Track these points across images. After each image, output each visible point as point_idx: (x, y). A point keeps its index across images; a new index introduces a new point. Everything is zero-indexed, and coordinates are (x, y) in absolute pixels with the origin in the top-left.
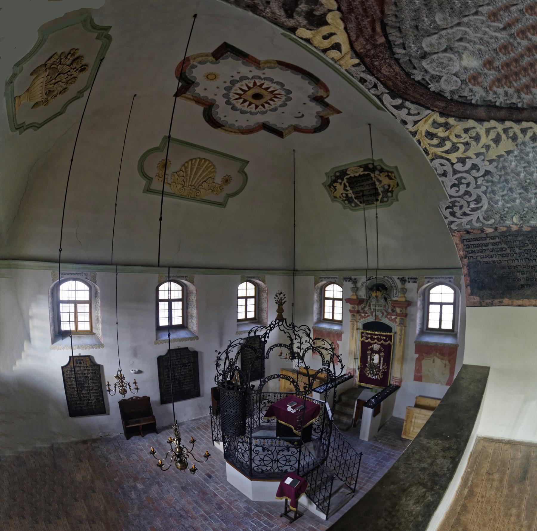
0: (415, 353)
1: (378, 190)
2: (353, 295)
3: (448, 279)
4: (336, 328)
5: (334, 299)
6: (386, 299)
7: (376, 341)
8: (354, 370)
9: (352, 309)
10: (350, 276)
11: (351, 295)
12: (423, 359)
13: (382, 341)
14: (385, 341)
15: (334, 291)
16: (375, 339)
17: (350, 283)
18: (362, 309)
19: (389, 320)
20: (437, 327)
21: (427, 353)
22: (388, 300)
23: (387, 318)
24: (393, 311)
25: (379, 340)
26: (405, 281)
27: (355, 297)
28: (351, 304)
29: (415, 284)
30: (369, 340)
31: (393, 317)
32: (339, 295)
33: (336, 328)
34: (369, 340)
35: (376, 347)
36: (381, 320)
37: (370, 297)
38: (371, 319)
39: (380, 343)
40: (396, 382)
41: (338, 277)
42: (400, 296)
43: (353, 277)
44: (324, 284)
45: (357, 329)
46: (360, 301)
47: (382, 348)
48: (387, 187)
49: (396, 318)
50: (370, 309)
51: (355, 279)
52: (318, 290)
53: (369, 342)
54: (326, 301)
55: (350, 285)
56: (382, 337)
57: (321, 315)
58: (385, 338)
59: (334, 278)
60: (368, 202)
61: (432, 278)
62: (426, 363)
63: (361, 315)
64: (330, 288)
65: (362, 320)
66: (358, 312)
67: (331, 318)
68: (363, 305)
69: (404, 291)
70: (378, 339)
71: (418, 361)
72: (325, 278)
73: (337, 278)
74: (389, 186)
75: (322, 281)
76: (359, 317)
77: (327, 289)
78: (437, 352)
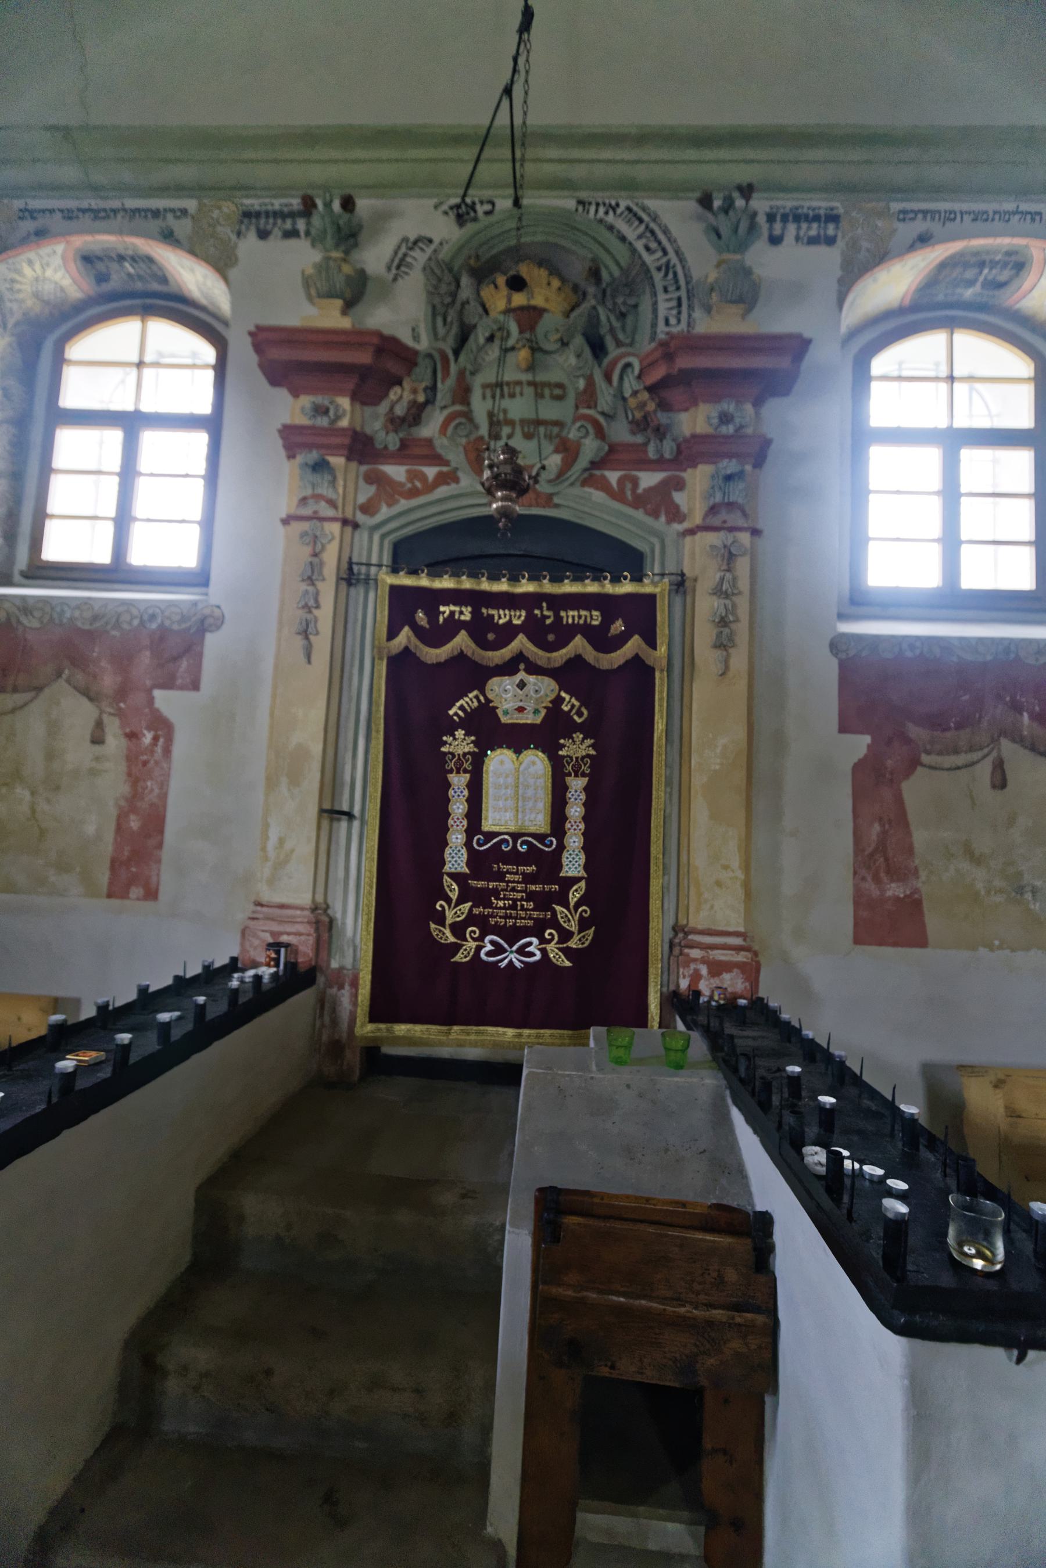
0: (844, 728)
7: (521, 643)
8: (324, 924)
13: (579, 644)
14: (601, 640)
16: (509, 632)
17: (301, 245)
19: (618, 495)
23: (604, 486)
30: (462, 641)
31: (648, 479)
34: (462, 641)
36: (548, 500)
40: (717, 969)
47: (569, 702)
50: (468, 415)
53: (460, 658)
56: (570, 616)
58: (596, 618)
59: (156, 214)
70: (535, 630)
76: (366, 493)
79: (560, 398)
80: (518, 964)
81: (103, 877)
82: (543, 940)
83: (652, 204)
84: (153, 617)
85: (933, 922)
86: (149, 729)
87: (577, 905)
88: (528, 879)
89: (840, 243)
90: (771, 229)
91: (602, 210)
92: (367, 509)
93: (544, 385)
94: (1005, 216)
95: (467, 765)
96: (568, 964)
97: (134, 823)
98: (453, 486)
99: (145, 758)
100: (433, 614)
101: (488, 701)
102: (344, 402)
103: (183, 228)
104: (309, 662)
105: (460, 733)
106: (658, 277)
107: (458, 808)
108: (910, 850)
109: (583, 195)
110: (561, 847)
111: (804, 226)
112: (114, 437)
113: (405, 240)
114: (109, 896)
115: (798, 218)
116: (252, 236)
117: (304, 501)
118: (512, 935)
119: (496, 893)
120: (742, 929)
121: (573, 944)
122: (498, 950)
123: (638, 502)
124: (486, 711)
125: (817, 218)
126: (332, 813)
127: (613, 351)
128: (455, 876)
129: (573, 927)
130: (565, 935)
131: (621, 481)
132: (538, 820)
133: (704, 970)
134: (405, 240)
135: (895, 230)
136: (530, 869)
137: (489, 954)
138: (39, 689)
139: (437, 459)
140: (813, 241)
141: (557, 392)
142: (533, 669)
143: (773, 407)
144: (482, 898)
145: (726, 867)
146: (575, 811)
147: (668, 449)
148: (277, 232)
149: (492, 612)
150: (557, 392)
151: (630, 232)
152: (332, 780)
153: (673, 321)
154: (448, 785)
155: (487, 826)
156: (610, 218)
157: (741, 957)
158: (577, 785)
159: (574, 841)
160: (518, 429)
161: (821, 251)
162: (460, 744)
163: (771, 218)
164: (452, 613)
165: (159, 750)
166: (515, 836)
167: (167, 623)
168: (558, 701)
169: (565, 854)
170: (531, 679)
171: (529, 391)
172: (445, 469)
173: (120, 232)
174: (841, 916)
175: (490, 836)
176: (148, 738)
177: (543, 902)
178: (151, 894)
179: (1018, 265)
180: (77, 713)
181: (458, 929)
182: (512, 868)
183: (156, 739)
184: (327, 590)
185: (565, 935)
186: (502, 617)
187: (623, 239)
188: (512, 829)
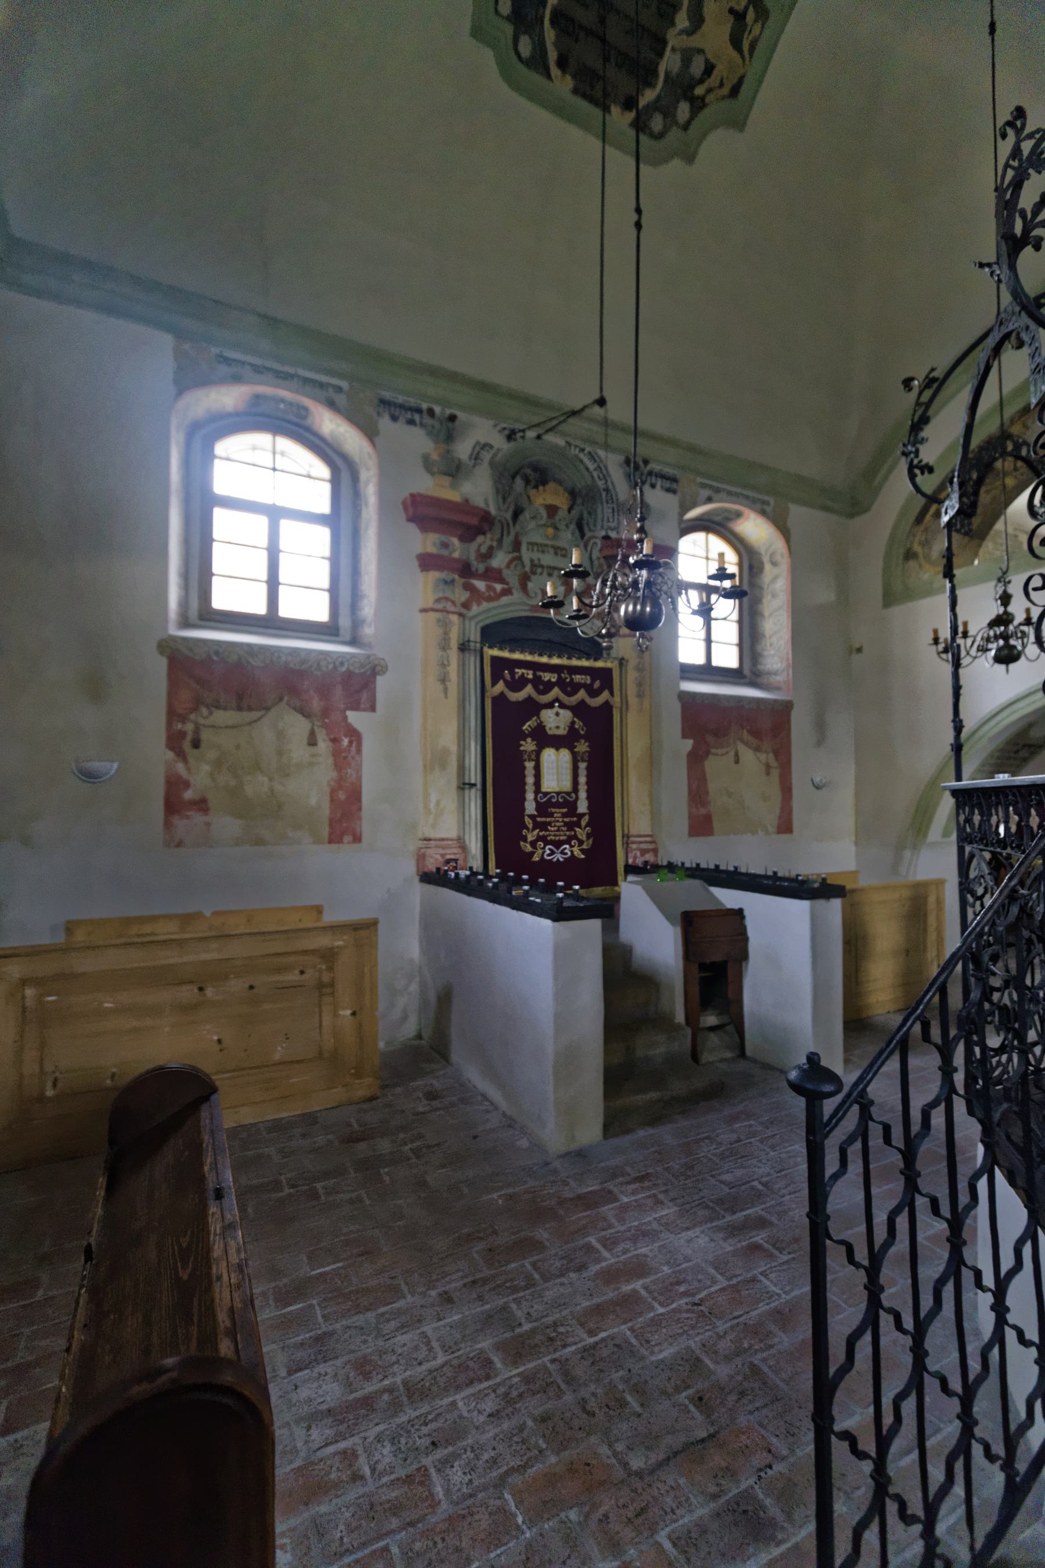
0: (685, 736)
1: (660, 54)
7: (556, 692)
13: (582, 694)
20: (700, 660)
25: (570, 689)
29: (670, 496)
34: (529, 690)
35: (556, 720)
37: (517, 513)
38: (514, 605)
39: (574, 700)
40: (644, 852)
48: (697, 68)
50: (520, 558)
53: (529, 699)
56: (578, 678)
58: (588, 680)
60: (593, 88)
61: (717, 490)
68: (483, 542)
70: (561, 684)
73: (339, 389)
74: (709, 69)
76: (465, 596)
78: (743, 728)
80: (561, 859)
81: (325, 831)
82: (571, 846)
84: (342, 664)
85: (716, 824)
86: (346, 736)
87: (586, 826)
88: (564, 815)
89: (679, 493)
94: (737, 495)
95: (533, 757)
96: (583, 856)
97: (341, 796)
98: (510, 597)
99: (344, 754)
100: (512, 674)
101: (541, 722)
102: (455, 541)
103: (341, 399)
104: (446, 697)
105: (529, 740)
107: (530, 780)
109: (569, 440)
110: (577, 798)
113: (478, 443)
114: (330, 842)
117: (438, 600)
118: (558, 844)
119: (550, 824)
120: (650, 833)
121: (584, 847)
122: (552, 853)
124: (540, 728)
126: (464, 786)
127: (588, 534)
128: (531, 817)
129: (584, 838)
130: (581, 843)
132: (567, 785)
133: (638, 853)
134: (478, 443)
136: (565, 810)
137: (549, 855)
138: (268, 709)
139: (502, 581)
140: (668, 490)
142: (562, 706)
144: (543, 826)
146: (582, 780)
149: (541, 674)
151: (591, 466)
152: (462, 768)
154: (524, 768)
155: (544, 789)
156: (581, 455)
158: (582, 765)
159: (583, 794)
160: (545, 572)
162: (528, 745)
164: (523, 674)
165: (353, 749)
166: (558, 793)
167: (352, 668)
168: (573, 723)
169: (579, 802)
170: (561, 711)
171: (552, 551)
172: (506, 586)
173: (297, 392)
174: (684, 824)
175: (546, 794)
176: (346, 742)
177: (570, 826)
178: (357, 839)
179: (739, 515)
180: (297, 726)
181: (533, 844)
182: (558, 810)
183: (351, 742)
184: (454, 654)
185: (581, 843)
186: (547, 676)
187: (587, 469)
188: (557, 790)
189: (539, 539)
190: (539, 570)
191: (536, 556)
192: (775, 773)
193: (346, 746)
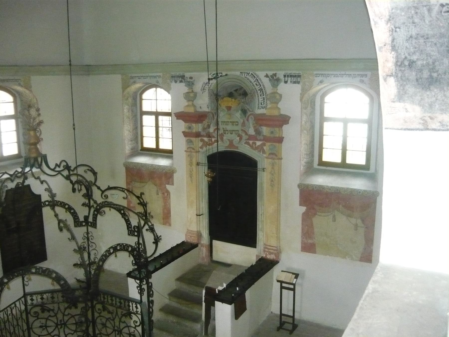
0: (301, 205)
2: (188, 106)
3: (358, 79)
4: (163, 162)
5: (157, 114)
6: (244, 112)
8: (199, 235)
9: (187, 131)
10: (181, 74)
11: (183, 106)
12: (315, 214)
15: (158, 99)
17: (183, 84)
18: (204, 129)
19: (252, 147)
20: (338, 160)
21: (321, 205)
22: (249, 113)
23: (248, 144)
24: (258, 132)
26: (278, 80)
27: (191, 110)
28: (185, 121)
31: (258, 143)
32: (166, 106)
33: (163, 162)
41: (161, 74)
42: (269, 106)
43: (187, 75)
44: (140, 88)
45: (198, 164)
46: (199, 117)
49: (264, 145)
51: (191, 78)
52: (130, 100)
54: (145, 117)
55: (182, 88)
57: (137, 143)
59: (155, 77)
62: (321, 222)
63: (202, 140)
64: (149, 94)
65: (204, 149)
66: (198, 135)
67: (154, 146)
68: (206, 122)
69: (276, 98)
71: (307, 218)
72: (139, 78)
75: (135, 82)
77: (145, 96)
78: (339, 203)
79: (237, 125)
83: (257, 73)
84: (164, 169)
85: (318, 249)
89: (301, 83)
90: (285, 79)
91: (246, 74)
92: (201, 148)
93: (233, 122)
106: (259, 92)
108: (313, 233)
111: (293, 78)
112: (153, 117)
113: (204, 83)
115: (291, 76)
116: (173, 82)
117: (188, 148)
123: (256, 148)
125: (295, 76)
131: (253, 143)
134: (204, 83)
135: (314, 80)
140: (295, 82)
141: (237, 123)
143: (285, 127)
145: (273, 233)
147: (261, 137)
148: (178, 81)
150: (237, 123)
153: (263, 104)
156: (248, 76)
157: (275, 252)
161: (297, 85)
163: (285, 76)
178: (170, 225)
184: (194, 167)
189: (226, 120)
190: (227, 132)
191: (224, 127)
192: (362, 231)
193: (166, 195)
